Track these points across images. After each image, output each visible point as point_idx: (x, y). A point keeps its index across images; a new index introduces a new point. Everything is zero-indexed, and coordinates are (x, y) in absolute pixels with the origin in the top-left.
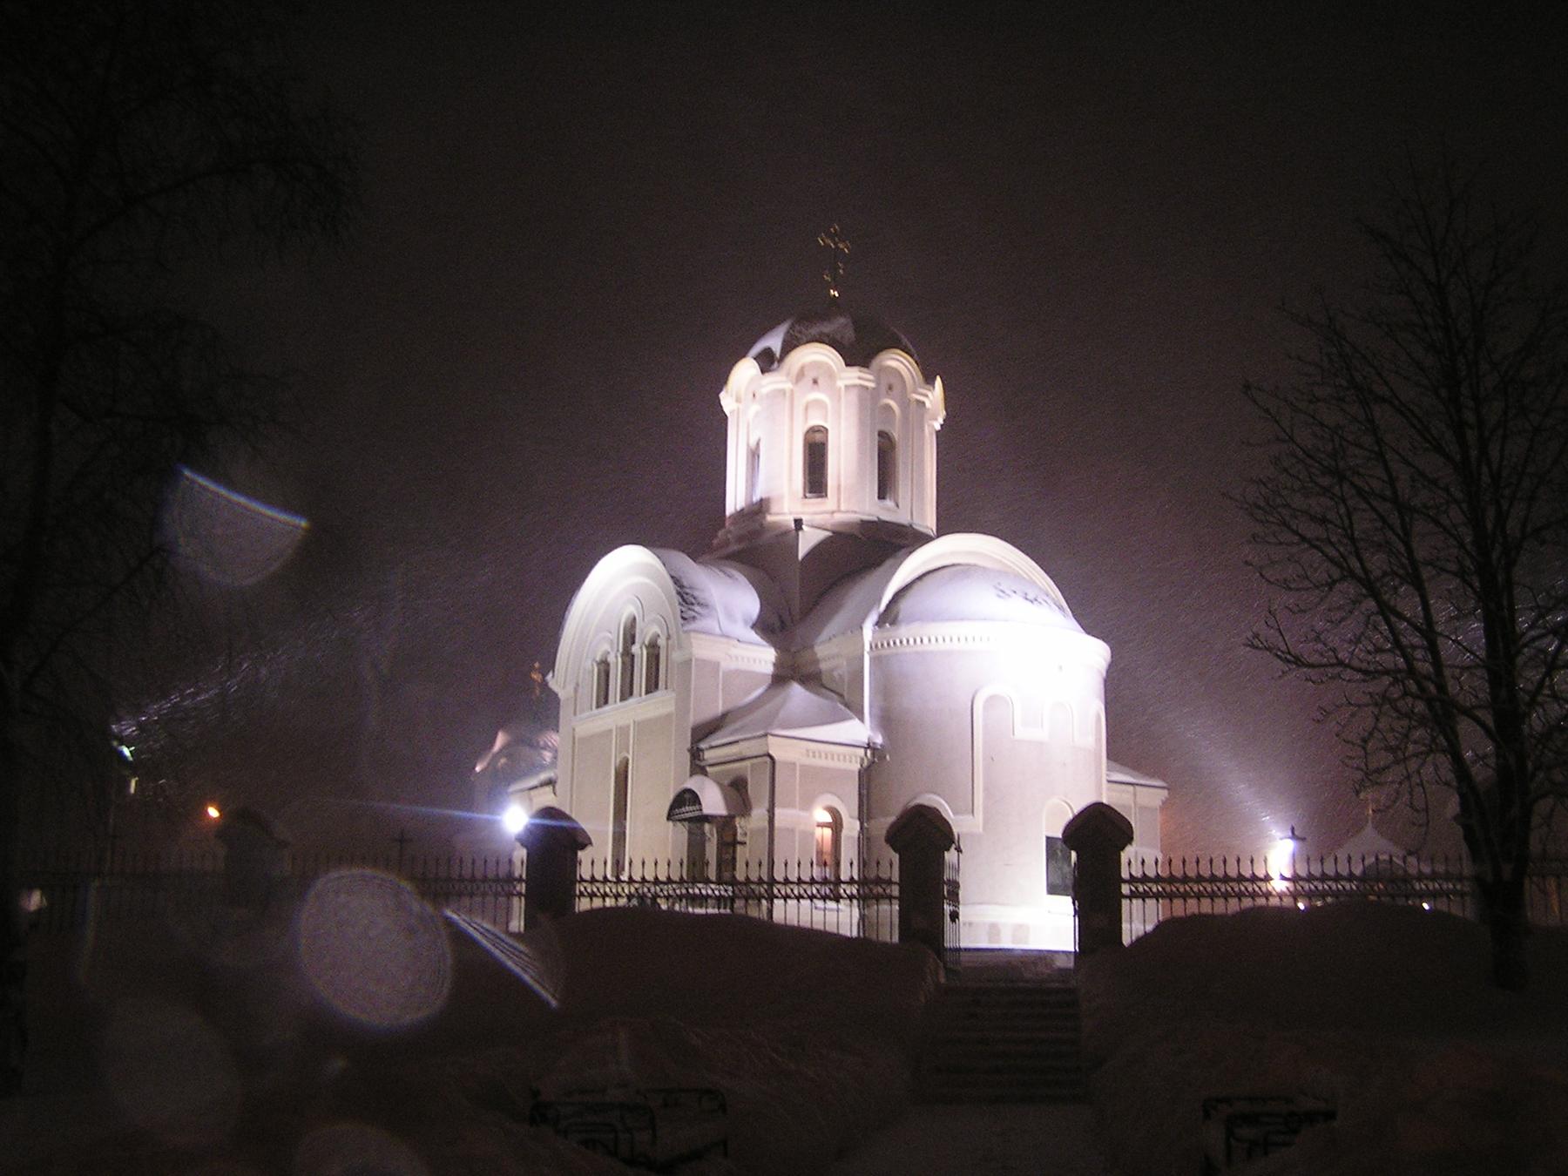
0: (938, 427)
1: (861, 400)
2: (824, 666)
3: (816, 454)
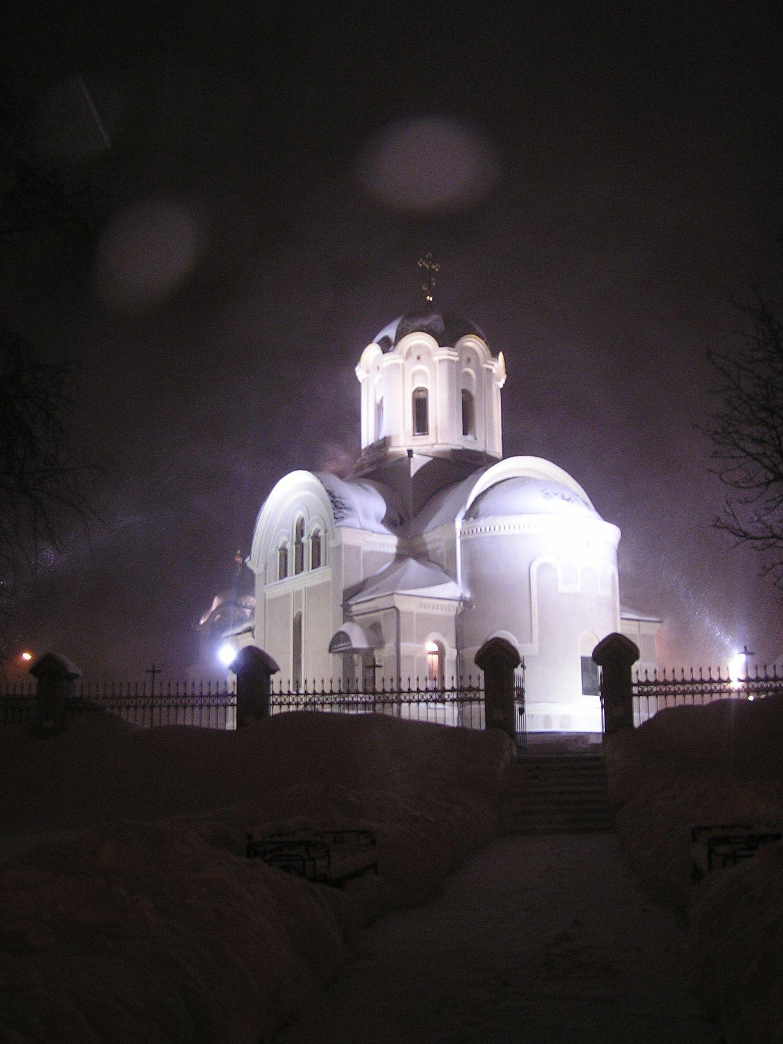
0: (501, 386)
1: (450, 371)
2: (429, 547)
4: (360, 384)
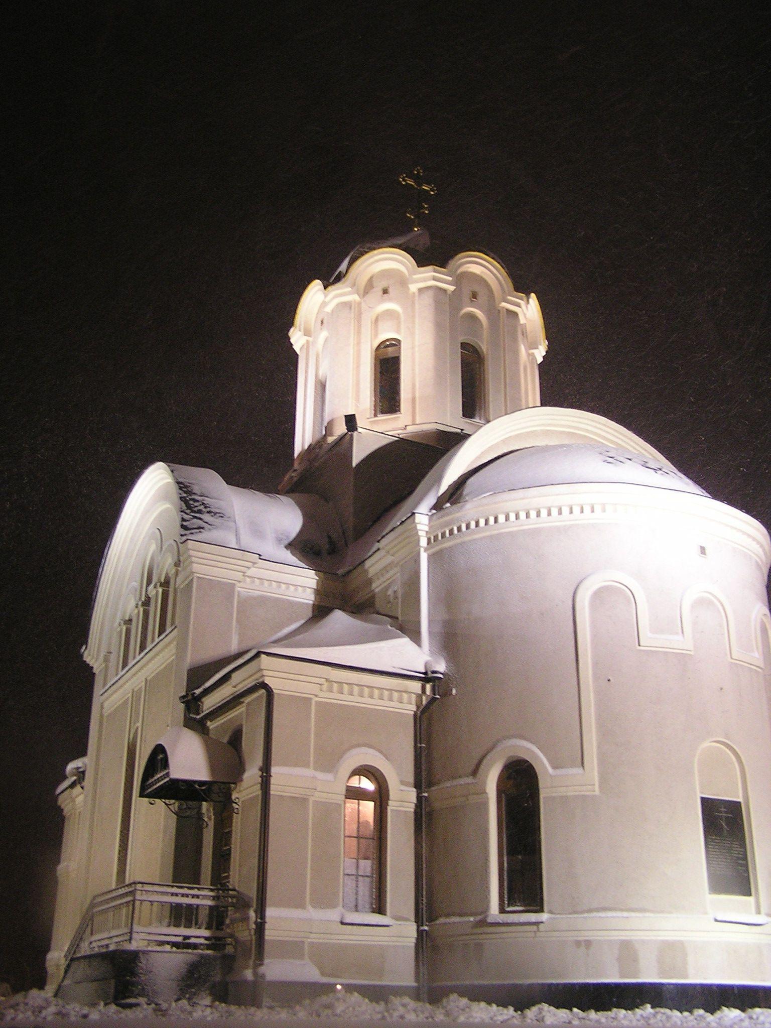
0: (540, 360)
3: (387, 368)
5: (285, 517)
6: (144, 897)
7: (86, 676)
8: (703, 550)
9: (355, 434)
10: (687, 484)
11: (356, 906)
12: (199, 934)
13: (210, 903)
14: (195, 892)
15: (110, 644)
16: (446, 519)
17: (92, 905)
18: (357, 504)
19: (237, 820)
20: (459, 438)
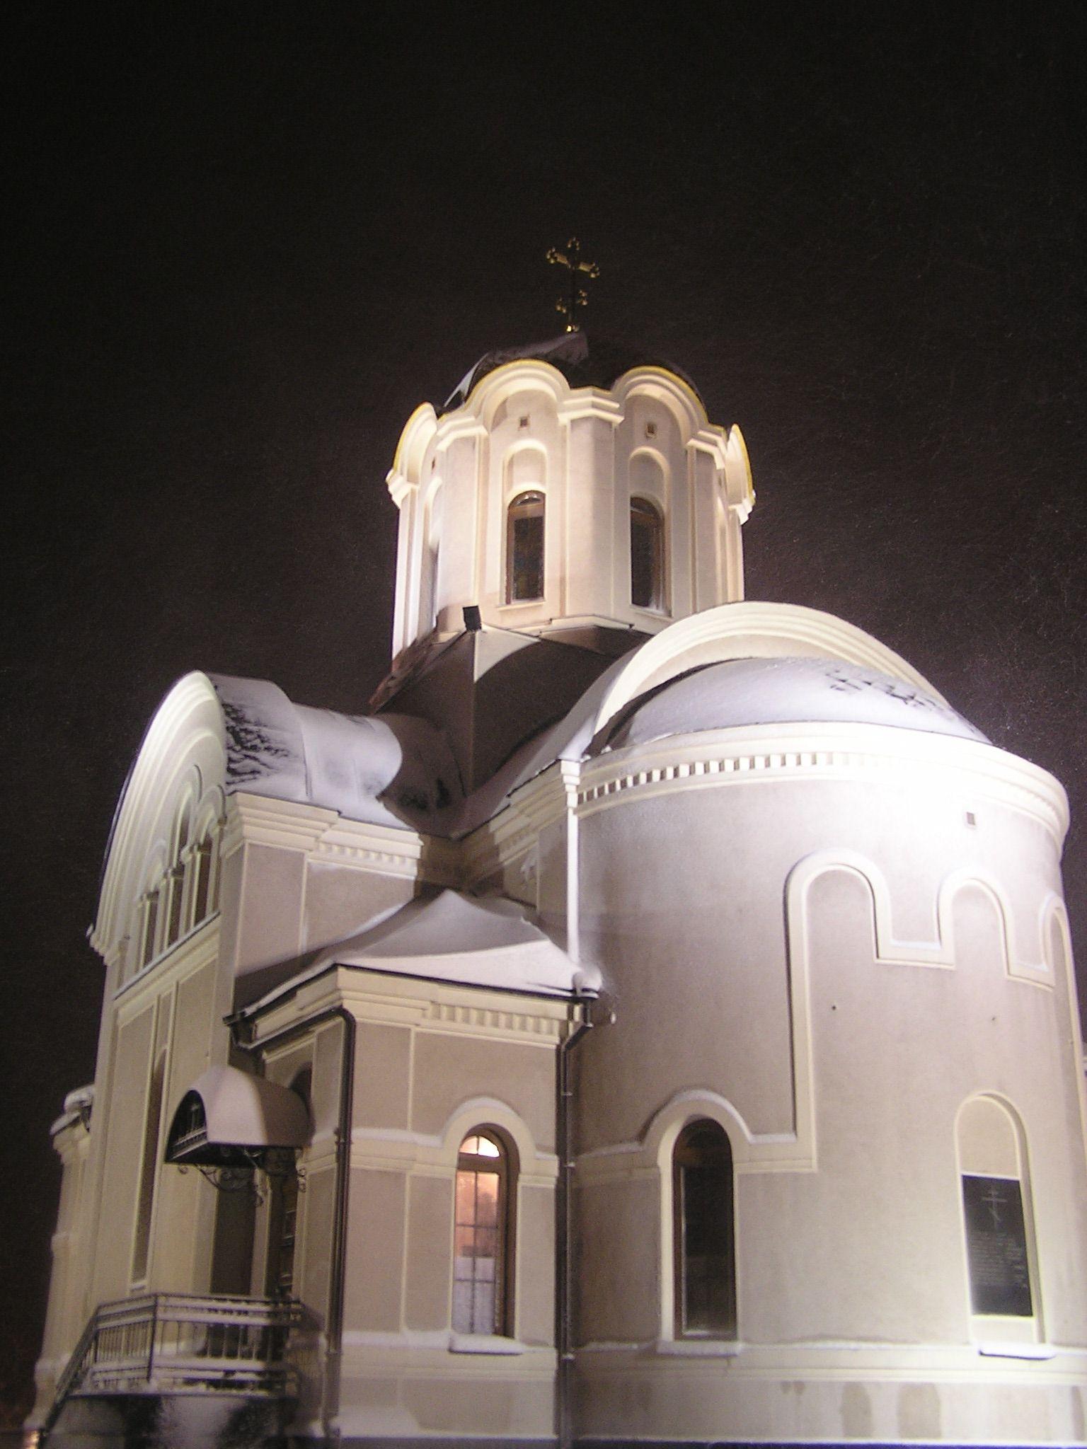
0: (744, 519)
2: (507, 858)
3: (526, 532)
4: (396, 511)
5: (377, 753)
6: (169, 1315)
7: (97, 967)
8: (971, 818)
9: (478, 634)
10: (950, 719)
11: (472, 1325)
12: (248, 1367)
13: (262, 1321)
14: (243, 1306)
15: (128, 922)
16: (602, 769)
17: (96, 1319)
18: (478, 733)
19: (303, 1200)
20: (624, 642)
